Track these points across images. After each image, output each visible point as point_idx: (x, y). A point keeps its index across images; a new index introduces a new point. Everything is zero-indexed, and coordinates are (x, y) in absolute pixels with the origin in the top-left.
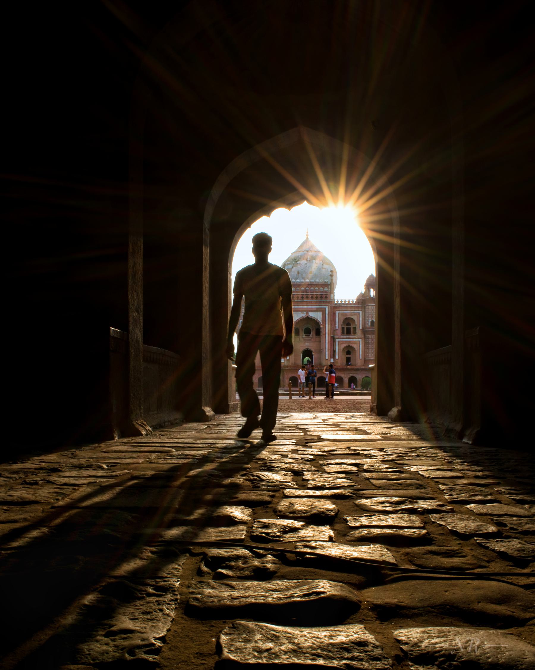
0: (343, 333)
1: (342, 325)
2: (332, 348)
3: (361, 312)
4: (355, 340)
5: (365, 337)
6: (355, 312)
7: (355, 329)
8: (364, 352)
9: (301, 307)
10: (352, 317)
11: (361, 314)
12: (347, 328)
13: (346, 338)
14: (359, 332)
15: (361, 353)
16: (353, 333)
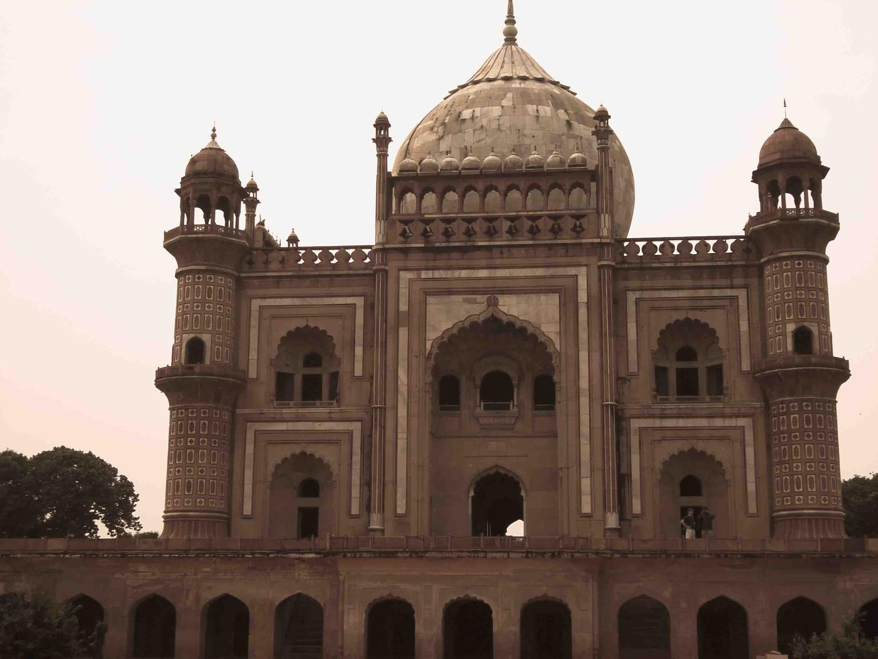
0: (661, 389)
1: (654, 353)
2: (611, 464)
3: (742, 294)
4: (718, 422)
5: (767, 407)
6: (716, 293)
7: (716, 372)
8: (768, 477)
9: (464, 273)
10: (703, 317)
11: (743, 303)
12: (678, 371)
13: (679, 416)
14: (738, 388)
15: (751, 487)
16: (710, 395)
